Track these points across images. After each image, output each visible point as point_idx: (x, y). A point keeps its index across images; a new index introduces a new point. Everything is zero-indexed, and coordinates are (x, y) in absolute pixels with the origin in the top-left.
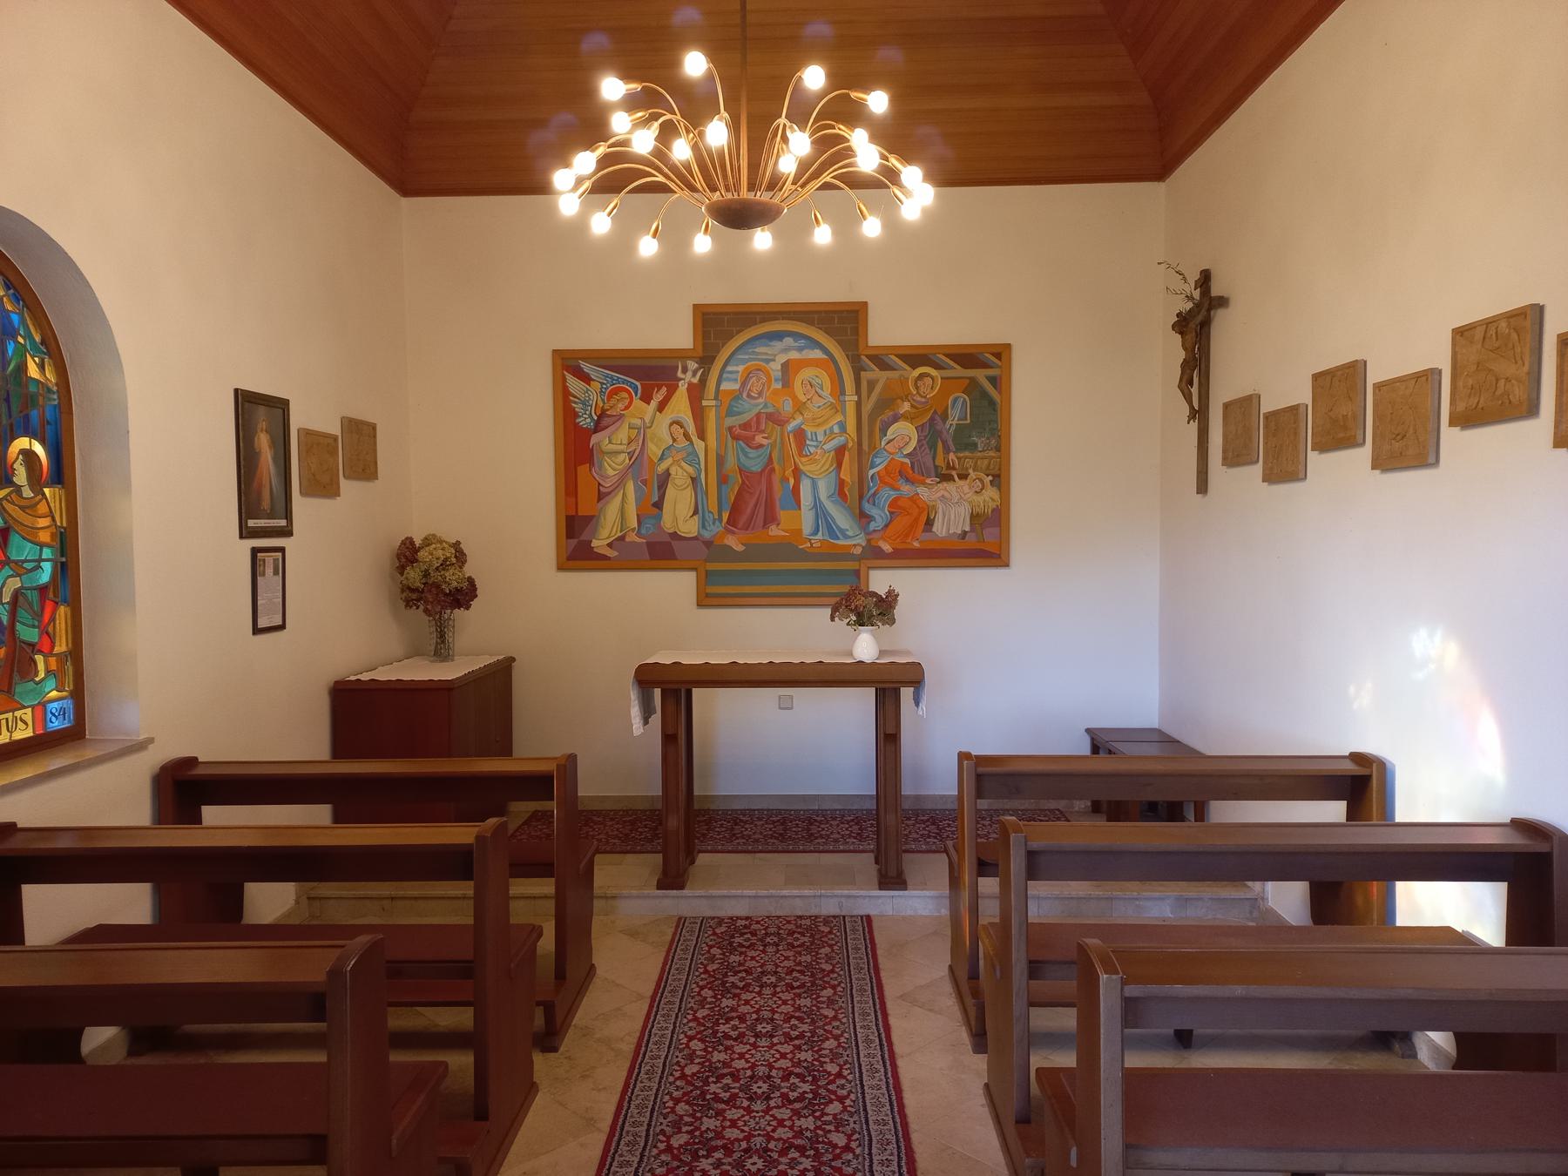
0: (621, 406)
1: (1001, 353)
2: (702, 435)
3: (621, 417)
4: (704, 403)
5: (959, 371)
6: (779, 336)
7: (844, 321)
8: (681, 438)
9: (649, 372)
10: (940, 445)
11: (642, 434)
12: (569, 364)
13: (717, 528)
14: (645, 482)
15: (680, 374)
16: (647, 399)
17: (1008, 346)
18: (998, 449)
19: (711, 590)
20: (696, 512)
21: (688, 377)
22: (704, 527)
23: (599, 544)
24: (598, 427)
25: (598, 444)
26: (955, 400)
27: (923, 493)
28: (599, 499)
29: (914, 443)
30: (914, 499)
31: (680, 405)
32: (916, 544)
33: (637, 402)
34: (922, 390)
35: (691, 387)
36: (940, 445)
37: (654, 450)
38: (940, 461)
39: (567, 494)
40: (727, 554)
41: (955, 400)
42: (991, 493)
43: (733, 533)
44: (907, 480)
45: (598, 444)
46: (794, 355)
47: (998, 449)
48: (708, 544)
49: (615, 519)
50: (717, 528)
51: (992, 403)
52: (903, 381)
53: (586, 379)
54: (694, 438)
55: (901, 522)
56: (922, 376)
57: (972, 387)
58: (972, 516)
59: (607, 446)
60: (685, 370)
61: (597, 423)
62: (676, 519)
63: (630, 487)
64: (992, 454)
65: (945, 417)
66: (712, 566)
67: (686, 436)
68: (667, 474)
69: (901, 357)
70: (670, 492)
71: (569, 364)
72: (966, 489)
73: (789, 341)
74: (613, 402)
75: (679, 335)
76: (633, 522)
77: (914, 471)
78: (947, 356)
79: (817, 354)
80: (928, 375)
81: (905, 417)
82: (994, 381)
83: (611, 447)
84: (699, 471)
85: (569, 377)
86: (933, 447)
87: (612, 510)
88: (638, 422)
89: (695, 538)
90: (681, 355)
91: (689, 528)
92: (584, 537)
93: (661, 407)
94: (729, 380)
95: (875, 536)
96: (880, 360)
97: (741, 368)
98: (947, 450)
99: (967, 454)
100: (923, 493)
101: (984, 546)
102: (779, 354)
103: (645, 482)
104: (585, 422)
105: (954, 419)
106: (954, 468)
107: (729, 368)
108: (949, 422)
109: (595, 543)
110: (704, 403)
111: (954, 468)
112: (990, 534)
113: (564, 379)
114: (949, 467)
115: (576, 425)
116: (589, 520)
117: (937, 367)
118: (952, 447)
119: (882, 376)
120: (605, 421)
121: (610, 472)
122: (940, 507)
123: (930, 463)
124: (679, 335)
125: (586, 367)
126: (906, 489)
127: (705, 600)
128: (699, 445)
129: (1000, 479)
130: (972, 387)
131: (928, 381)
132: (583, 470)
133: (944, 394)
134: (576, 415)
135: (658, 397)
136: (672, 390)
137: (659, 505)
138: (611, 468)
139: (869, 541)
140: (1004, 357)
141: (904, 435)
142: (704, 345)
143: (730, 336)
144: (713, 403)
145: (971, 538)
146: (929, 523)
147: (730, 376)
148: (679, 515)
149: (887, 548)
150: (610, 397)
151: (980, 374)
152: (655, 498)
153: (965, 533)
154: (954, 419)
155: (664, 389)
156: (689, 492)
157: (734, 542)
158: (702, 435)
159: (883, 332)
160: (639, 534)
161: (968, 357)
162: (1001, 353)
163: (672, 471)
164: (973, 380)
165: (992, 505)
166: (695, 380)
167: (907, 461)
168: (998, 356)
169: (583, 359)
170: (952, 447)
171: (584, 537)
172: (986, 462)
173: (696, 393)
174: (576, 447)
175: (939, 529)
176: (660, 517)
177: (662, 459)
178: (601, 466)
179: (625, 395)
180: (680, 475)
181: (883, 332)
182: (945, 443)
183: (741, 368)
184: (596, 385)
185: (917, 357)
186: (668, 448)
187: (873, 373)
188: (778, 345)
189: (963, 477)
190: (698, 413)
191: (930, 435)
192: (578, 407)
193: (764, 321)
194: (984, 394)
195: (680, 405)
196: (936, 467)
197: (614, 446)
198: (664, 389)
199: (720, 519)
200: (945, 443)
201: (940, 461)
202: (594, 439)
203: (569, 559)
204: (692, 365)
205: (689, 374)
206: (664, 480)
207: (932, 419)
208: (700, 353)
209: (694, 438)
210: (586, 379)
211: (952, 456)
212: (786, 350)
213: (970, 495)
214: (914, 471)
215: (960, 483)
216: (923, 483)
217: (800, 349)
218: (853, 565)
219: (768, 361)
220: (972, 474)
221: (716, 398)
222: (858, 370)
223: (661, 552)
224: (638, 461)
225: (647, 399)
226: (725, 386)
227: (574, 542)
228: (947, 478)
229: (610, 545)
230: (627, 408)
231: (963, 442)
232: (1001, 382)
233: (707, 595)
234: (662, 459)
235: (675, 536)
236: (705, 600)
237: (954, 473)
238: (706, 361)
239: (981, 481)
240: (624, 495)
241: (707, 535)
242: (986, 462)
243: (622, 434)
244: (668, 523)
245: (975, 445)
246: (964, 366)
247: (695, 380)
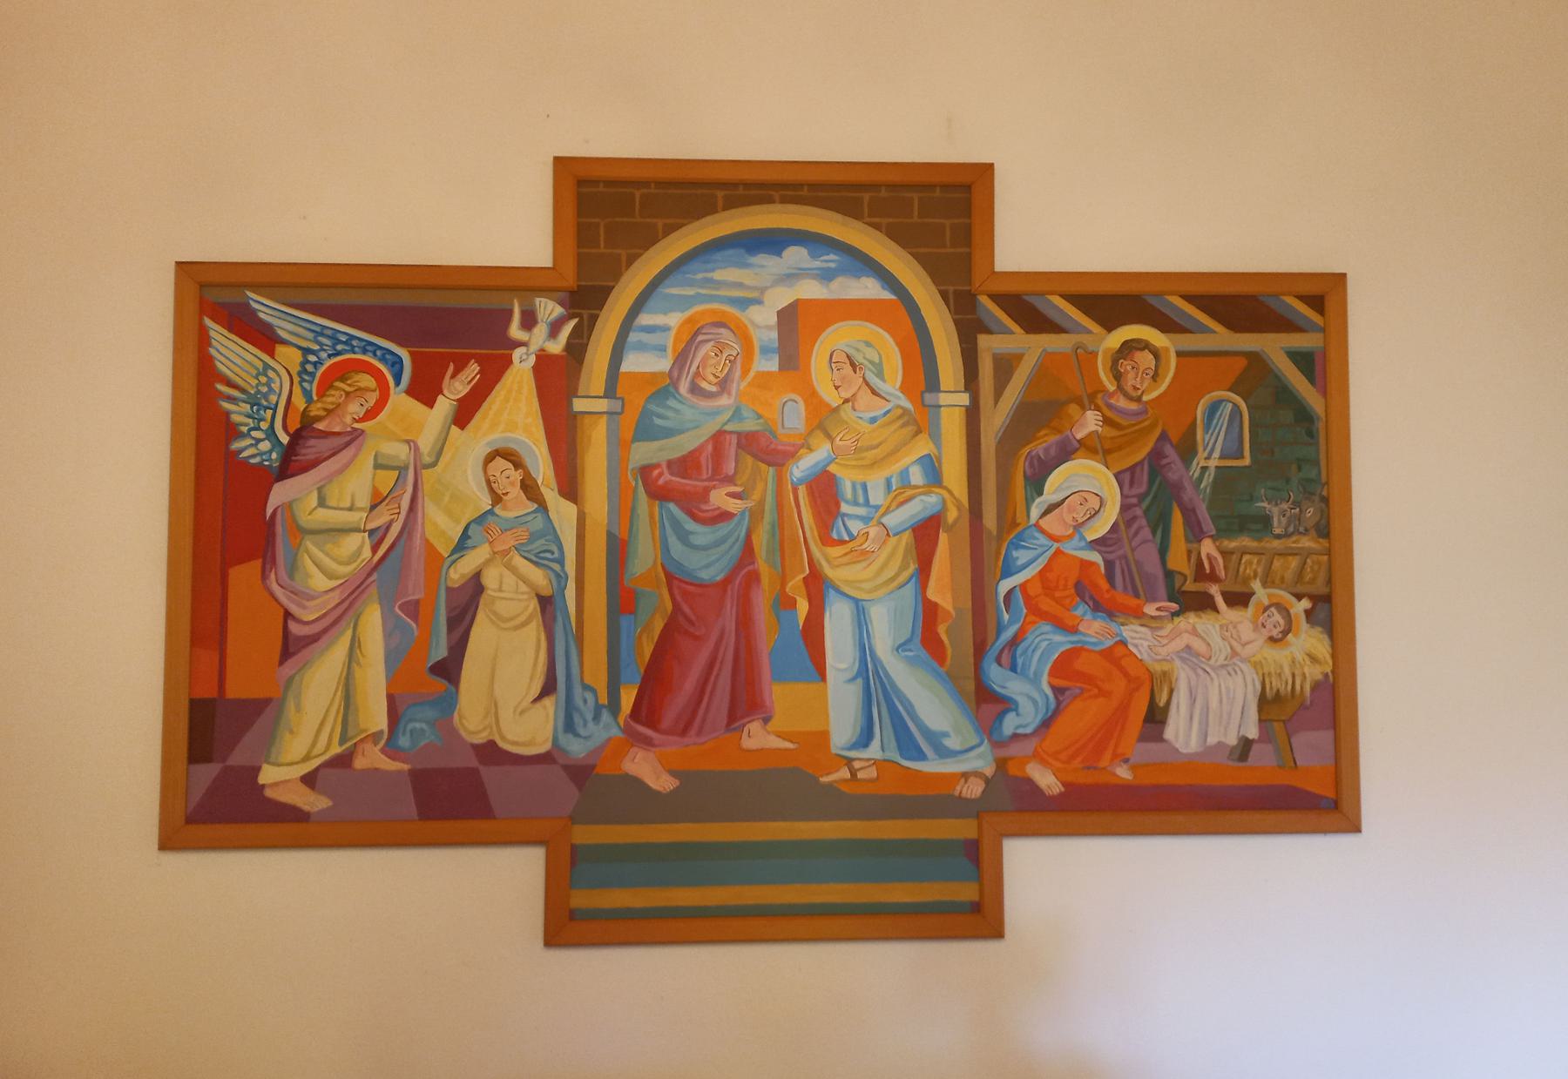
0: (355, 409)
1: (1323, 295)
2: (570, 488)
3: (355, 436)
4: (579, 405)
5: (1221, 338)
6: (772, 242)
7: (937, 210)
8: (516, 492)
9: (436, 326)
10: (1177, 518)
11: (409, 482)
12: (217, 299)
13: (600, 732)
14: (413, 609)
15: (515, 331)
16: (425, 392)
17: (1340, 279)
18: (1323, 531)
19: (581, 899)
20: (548, 689)
21: (538, 338)
22: (569, 727)
23: (279, 775)
24: (291, 464)
25: (289, 506)
26: (1214, 408)
27: (1138, 637)
28: (286, 653)
29: (1111, 514)
30: (1117, 655)
31: (514, 411)
32: (1124, 773)
33: (399, 399)
34: (1130, 381)
35: (544, 364)
36: (1177, 518)
37: (441, 525)
38: (1178, 560)
39: (196, 639)
40: (638, 802)
41: (1214, 408)
42: (1309, 642)
43: (648, 743)
44: (1097, 607)
45: (289, 506)
46: (811, 290)
47: (1323, 531)
48: (580, 773)
49: (327, 707)
50: (600, 732)
51: (1304, 416)
52: (1084, 359)
53: (265, 339)
54: (551, 495)
55: (1086, 715)
56: (1129, 348)
57: (1254, 377)
58: (1264, 702)
59: (310, 513)
60: (529, 321)
61: (289, 453)
62: (493, 708)
63: (372, 621)
64: (1306, 543)
65: (1188, 450)
66: (585, 835)
67: (529, 488)
68: (475, 586)
69: (1076, 300)
70: (482, 634)
71: (217, 299)
72: (1246, 630)
73: (796, 255)
74: (333, 397)
75: (516, 232)
76: (376, 717)
77: (1111, 584)
78: (1189, 298)
79: (868, 289)
80: (1143, 345)
81: (1089, 447)
82: (1306, 362)
83: (324, 516)
84: (561, 578)
85: (217, 332)
86: (1160, 523)
87: (318, 682)
88: (401, 452)
89: (545, 759)
90: (521, 282)
91: (529, 728)
92: (238, 758)
93: (464, 414)
94: (642, 347)
95: (1014, 750)
96: (1027, 306)
97: (674, 320)
98: (1196, 533)
99: (1245, 541)
100: (1138, 637)
101: (1295, 778)
102: (774, 286)
103: (413, 609)
104: (256, 449)
105: (1210, 456)
106: (1213, 578)
107: (645, 319)
108: (1199, 461)
109: (268, 775)
110: (579, 405)
111: (1213, 578)
112: (1311, 747)
113: (204, 340)
114: (1201, 574)
115: (233, 462)
116: (258, 713)
117: (1167, 324)
118: (1209, 526)
119: (1032, 347)
120: (313, 447)
121: (320, 582)
122: (1183, 677)
123: (1153, 566)
124: (516, 232)
125: (266, 308)
126: (1095, 630)
127: (566, 926)
128: (563, 512)
129: (1330, 606)
130: (1254, 377)
131: (1145, 359)
132: (243, 576)
133: (1184, 392)
134: (233, 432)
135: (457, 387)
136: (494, 370)
137: (449, 670)
138: (321, 570)
139: (1001, 764)
140: (1330, 305)
141: (1087, 491)
142: (581, 261)
143: (650, 240)
144: (602, 405)
145: (1263, 757)
146: (1156, 718)
147: (649, 333)
148: (506, 695)
149: (1047, 780)
150: (325, 386)
151: (1274, 347)
152: (440, 651)
153: (1246, 745)
154: (1210, 456)
155: (473, 369)
156: (533, 634)
157: (647, 769)
158: (570, 488)
159: (1033, 236)
160: (391, 751)
161: (1241, 303)
162: (1323, 295)
163: (490, 579)
164: (1255, 360)
165: (1314, 673)
166: (556, 347)
167: (1095, 557)
168: (1317, 302)
169: (257, 287)
170: (1209, 526)
171: (238, 758)
172: (1294, 563)
173: (556, 380)
174: (228, 514)
175: (1183, 734)
176: (449, 703)
177: (462, 545)
178: (293, 568)
179: (367, 381)
180: (511, 589)
181: (1033, 236)
182: (1189, 514)
183: (674, 320)
184: (289, 356)
185: (1116, 301)
186: (481, 519)
187: (1006, 339)
188: (768, 265)
189: (1239, 599)
190: (563, 432)
191: (1153, 492)
192: (239, 413)
193: (731, 204)
194: (1284, 395)
195: (514, 411)
196: (1169, 575)
197: (328, 514)
198: (473, 369)
199: (614, 706)
200: (1189, 514)
201: (1178, 560)
202: (280, 494)
203: (189, 820)
204: (549, 309)
205: (541, 330)
206: (467, 603)
207: (1156, 455)
208: (570, 281)
209: (551, 495)
210: (265, 339)
211: (1207, 547)
212: (790, 278)
213: (1255, 645)
214: (1111, 584)
215: (1228, 614)
216: (1138, 614)
217: (826, 276)
218: (963, 829)
219: (744, 303)
220: (1261, 594)
221: (610, 392)
222: (969, 329)
223: (450, 797)
224: (394, 552)
225: (425, 392)
226: (633, 363)
227: (207, 773)
228: (1203, 603)
229: (309, 780)
230: (371, 414)
231: (1236, 514)
232: (1322, 365)
233: (573, 915)
234: (462, 545)
235: (490, 752)
236: (566, 926)
237: (1214, 590)
238: (585, 301)
239: (1284, 611)
240: (355, 644)
241: (577, 749)
242: (1294, 563)
243: (355, 482)
244: (472, 719)
245: (1265, 521)
246: (1234, 325)
247: (556, 347)
